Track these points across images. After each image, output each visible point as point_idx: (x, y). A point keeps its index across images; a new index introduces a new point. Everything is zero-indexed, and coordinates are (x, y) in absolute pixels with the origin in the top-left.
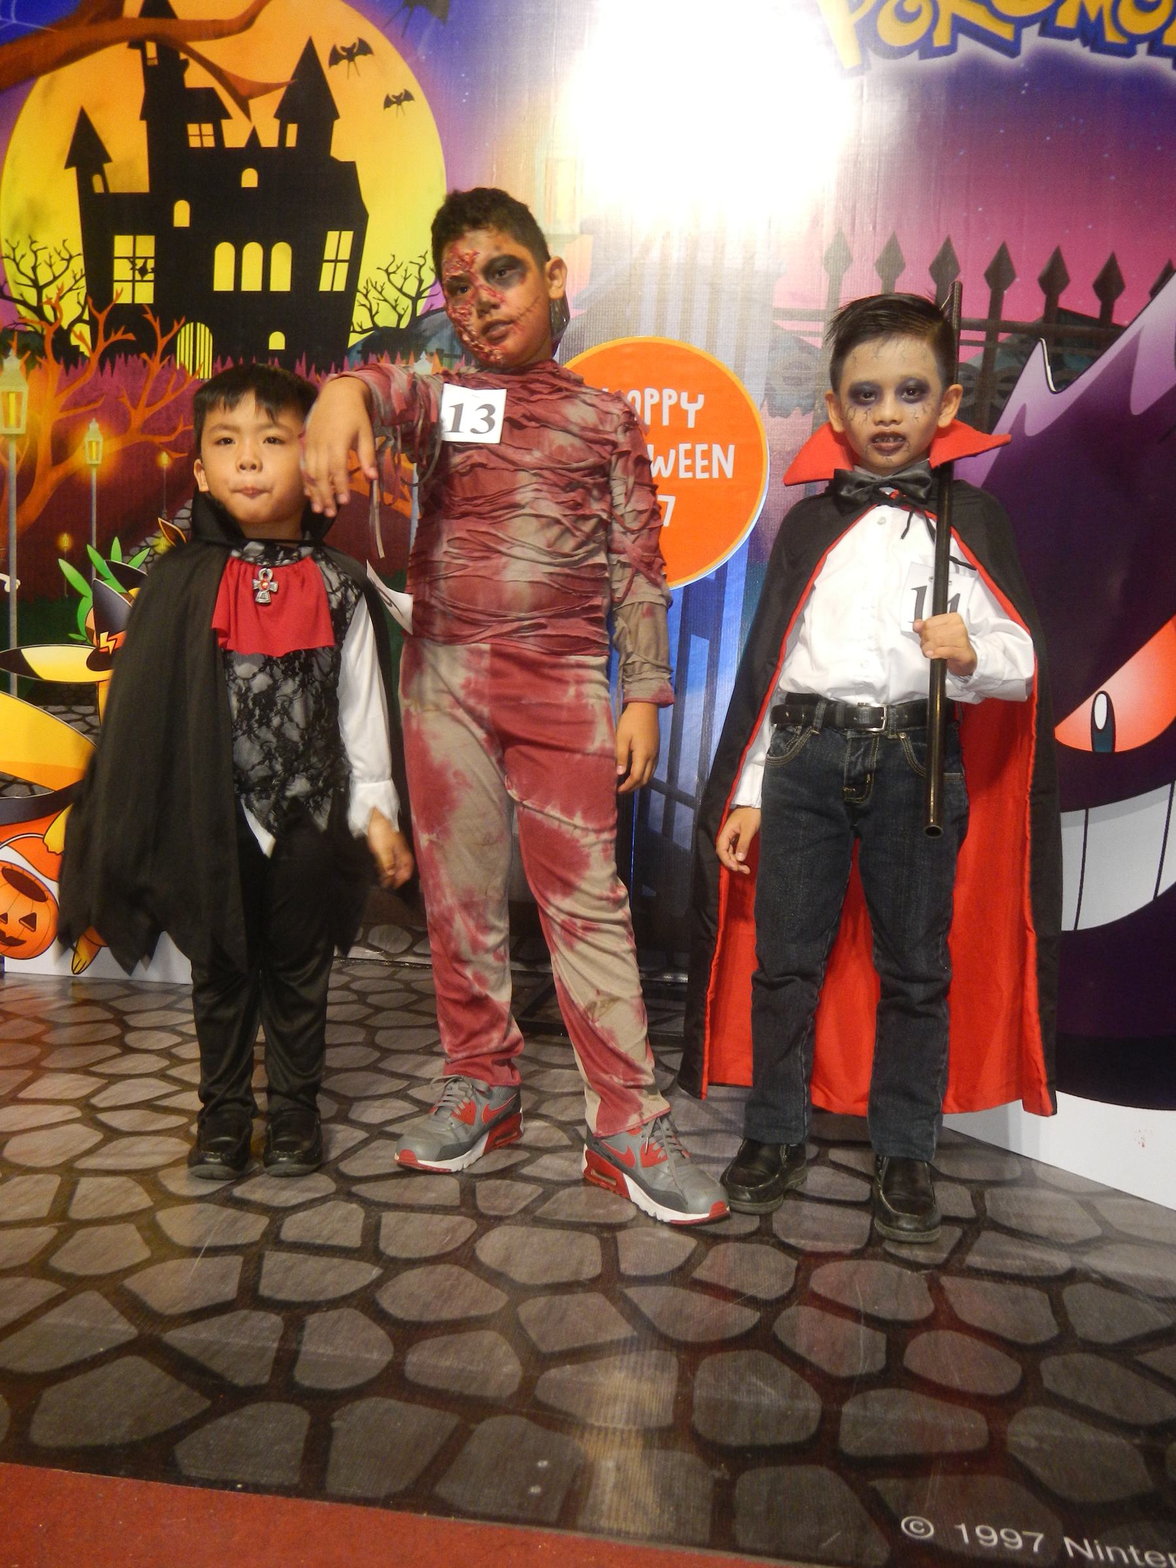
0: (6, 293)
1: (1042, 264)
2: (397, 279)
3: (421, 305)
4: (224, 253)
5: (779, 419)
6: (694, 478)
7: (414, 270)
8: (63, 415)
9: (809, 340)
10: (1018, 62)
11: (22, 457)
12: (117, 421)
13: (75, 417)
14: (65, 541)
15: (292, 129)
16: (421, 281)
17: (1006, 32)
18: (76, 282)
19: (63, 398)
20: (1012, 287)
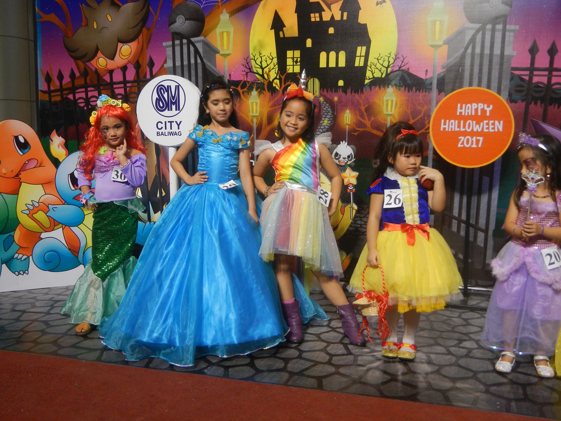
0: (252, 71)
2: (381, 62)
3: (389, 70)
4: (323, 55)
5: (513, 104)
6: (489, 132)
7: (386, 58)
9: (524, 77)
11: (258, 123)
13: (275, 109)
15: (345, 14)
16: (389, 62)
18: (275, 66)
19: (271, 104)
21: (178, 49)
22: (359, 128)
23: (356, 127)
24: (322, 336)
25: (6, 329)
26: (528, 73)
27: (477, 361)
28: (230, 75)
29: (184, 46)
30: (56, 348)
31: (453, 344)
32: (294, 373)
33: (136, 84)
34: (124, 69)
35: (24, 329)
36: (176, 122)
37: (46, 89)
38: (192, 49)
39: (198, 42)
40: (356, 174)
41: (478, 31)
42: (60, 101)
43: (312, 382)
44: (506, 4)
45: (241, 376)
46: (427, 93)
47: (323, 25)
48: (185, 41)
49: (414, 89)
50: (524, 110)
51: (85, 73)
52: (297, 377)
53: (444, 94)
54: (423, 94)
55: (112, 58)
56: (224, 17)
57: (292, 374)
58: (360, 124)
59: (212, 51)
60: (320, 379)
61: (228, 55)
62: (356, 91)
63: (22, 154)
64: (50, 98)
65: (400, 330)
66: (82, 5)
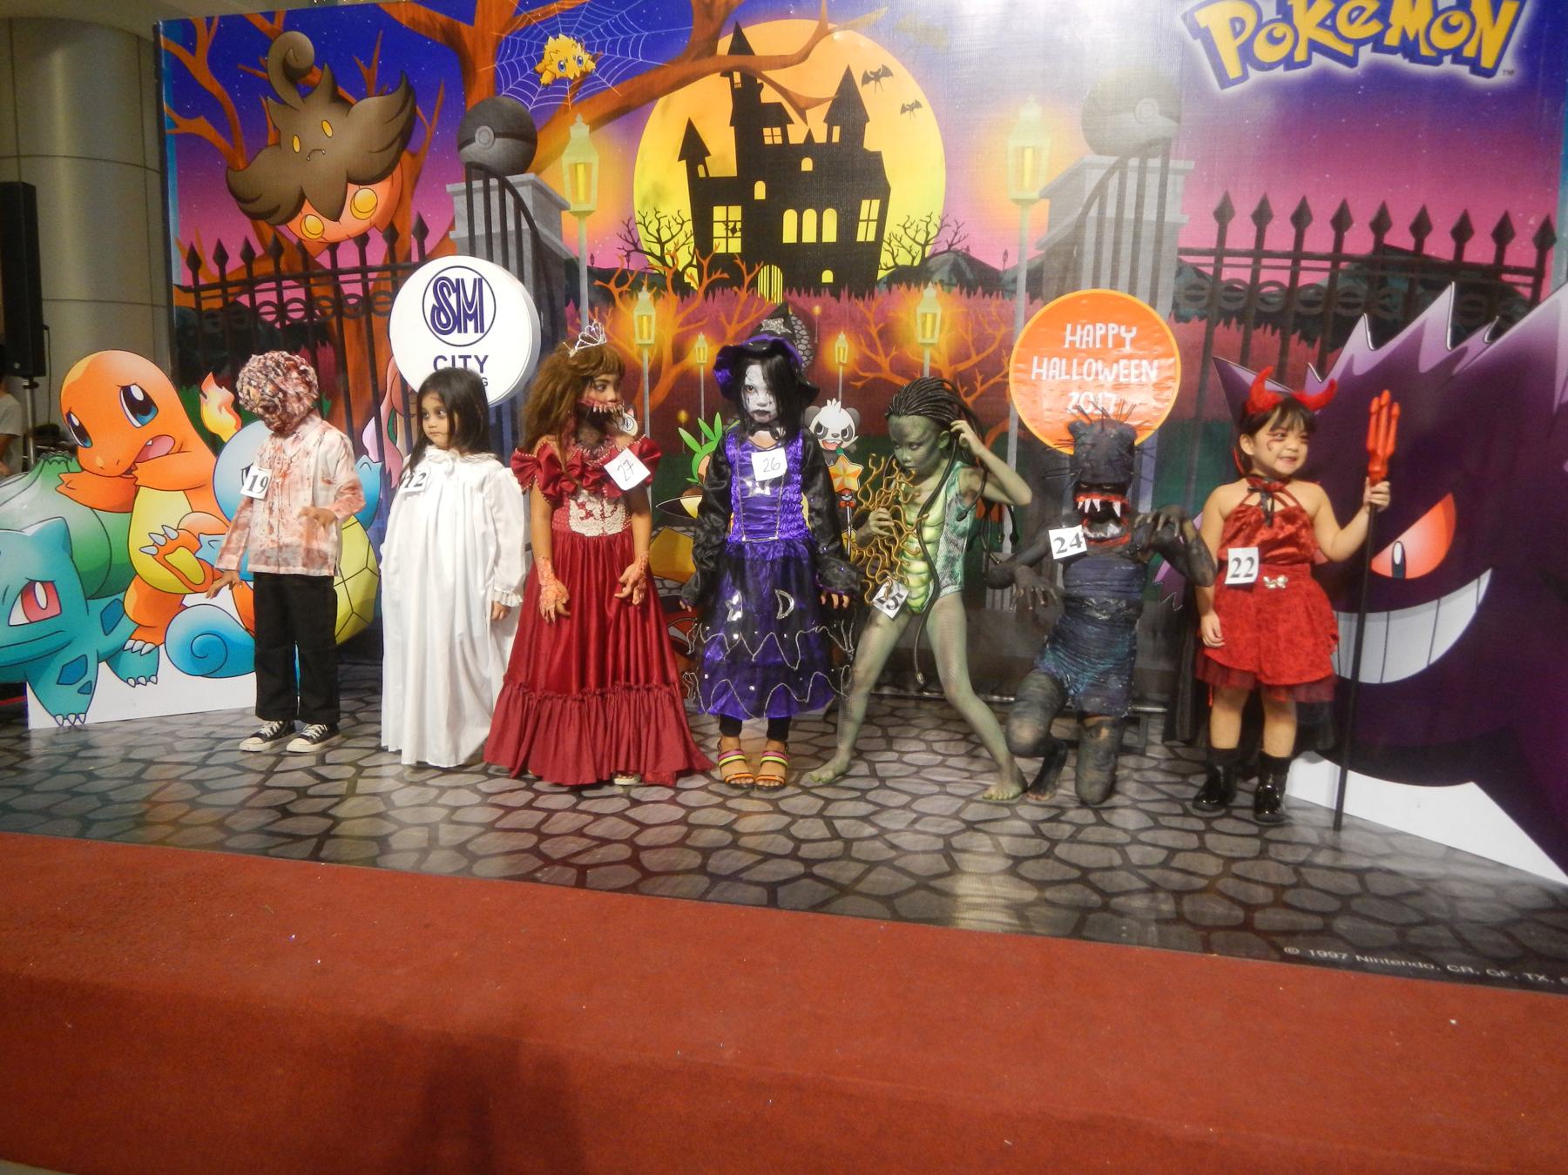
1: (1372, 214)
2: (911, 232)
3: (928, 250)
4: (790, 217)
5: (1182, 324)
7: (922, 225)
8: (679, 331)
11: (652, 359)
12: (717, 331)
13: (688, 331)
14: (683, 416)
15: (836, 130)
16: (928, 234)
17: (1347, 50)
19: (680, 318)
20: (1349, 231)
21: (478, 199)
22: (865, 371)
23: (861, 369)
24: (783, 805)
25: (112, 798)
26: (1211, 260)
27: (1091, 848)
28: (592, 257)
29: (492, 194)
30: (223, 836)
31: (1046, 816)
32: (721, 876)
33: (388, 274)
34: (362, 240)
35: (153, 798)
36: (477, 357)
37: (189, 282)
38: (509, 199)
39: (523, 184)
40: (857, 468)
41: (1110, 172)
42: (221, 309)
43: (758, 893)
44: (1171, 117)
45: (613, 884)
46: (1007, 299)
47: (789, 154)
48: (494, 182)
49: (980, 290)
50: (1202, 338)
51: (276, 250)
52: (724, 884)
53: (1042, 302)
54: (998, 302)
55: (336, 216)
56: (579, 130)
57: (716, 878)
58: (867, 363)
59: (553, 204)
60: (772, 888)
61: (588, 213)
62: (860, 295)
63: (138, 425)
64: (199, 304)
65: (943, 789)
66: (266, 99)
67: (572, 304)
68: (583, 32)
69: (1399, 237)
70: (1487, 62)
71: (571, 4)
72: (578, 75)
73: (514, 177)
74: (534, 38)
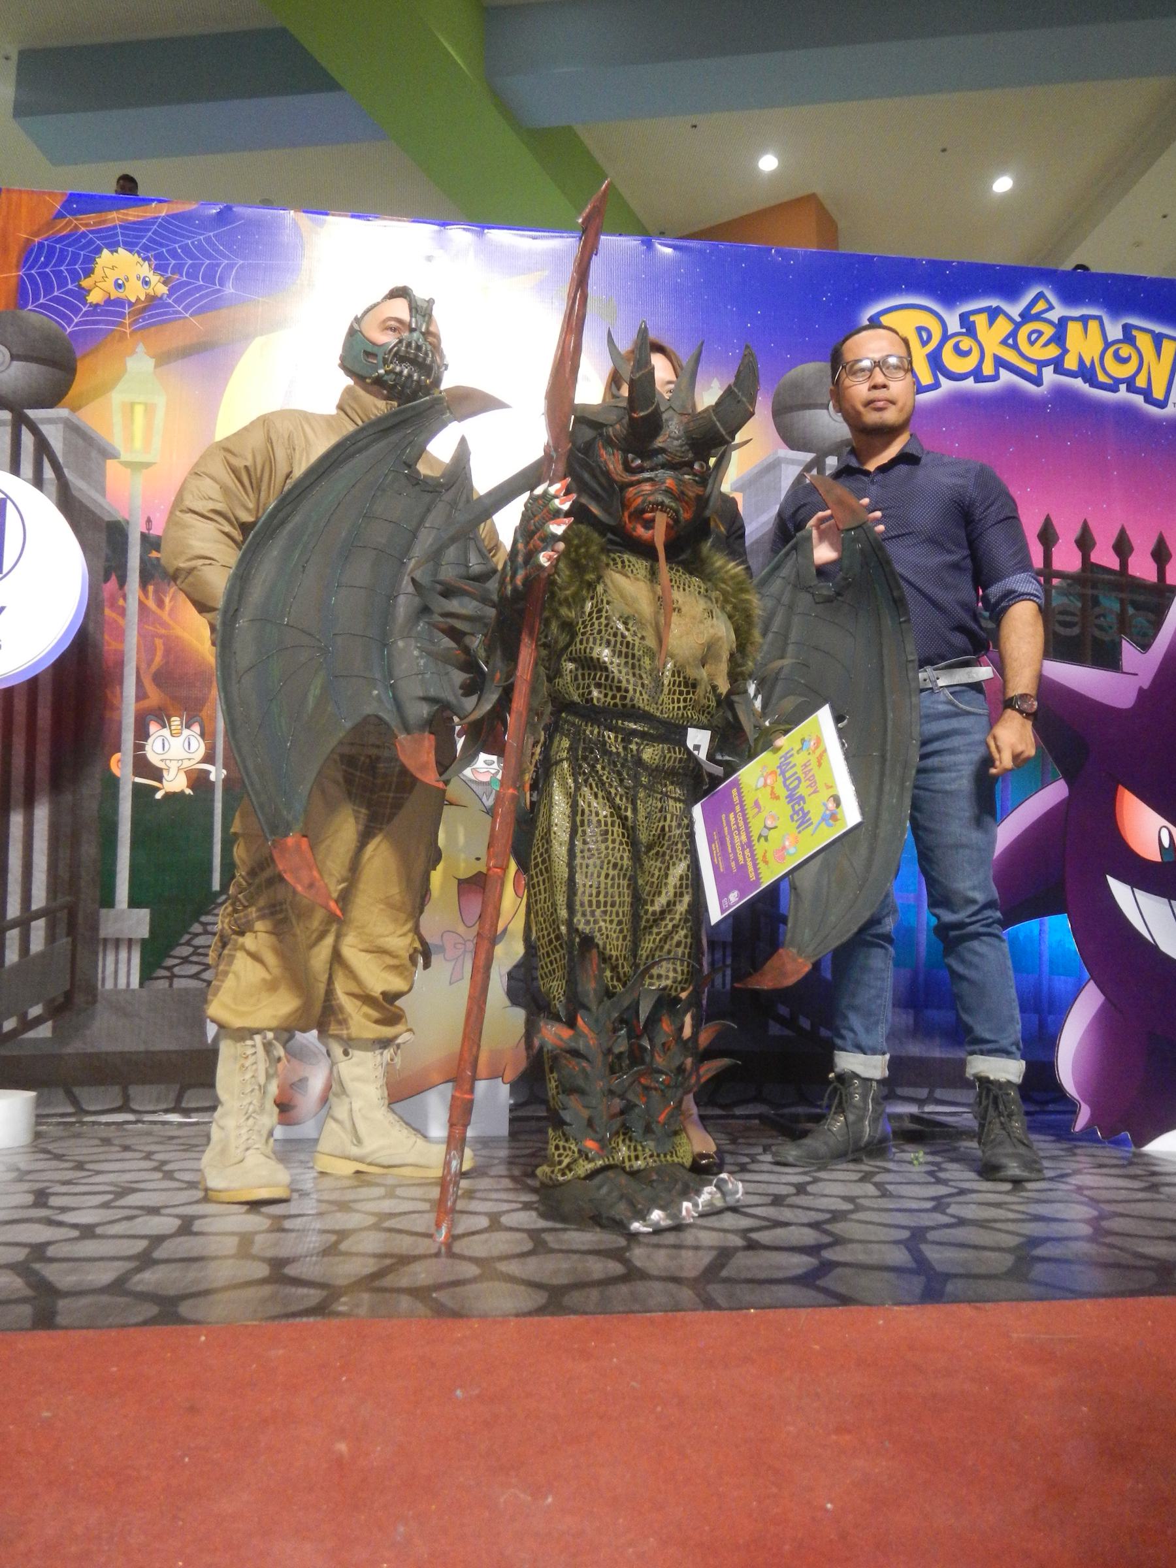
1: (1077, 532)
10: (1042, 390)
17: (1032, 369)
20: (1057, 546)
28: (149, 521)
38: (27, 438)
39: (50, 421)
61: (147, 465)
67: (114, 578)
68: (156, 249)
69: (1104, 556)
70: (1158, 393)
71: (134, 216)
72: (143, 298)
73: (36, 411)
74: (83, 248)
